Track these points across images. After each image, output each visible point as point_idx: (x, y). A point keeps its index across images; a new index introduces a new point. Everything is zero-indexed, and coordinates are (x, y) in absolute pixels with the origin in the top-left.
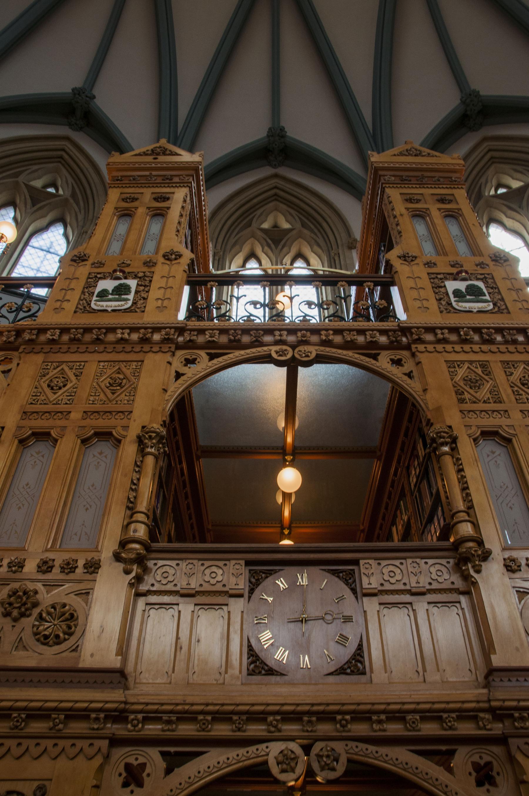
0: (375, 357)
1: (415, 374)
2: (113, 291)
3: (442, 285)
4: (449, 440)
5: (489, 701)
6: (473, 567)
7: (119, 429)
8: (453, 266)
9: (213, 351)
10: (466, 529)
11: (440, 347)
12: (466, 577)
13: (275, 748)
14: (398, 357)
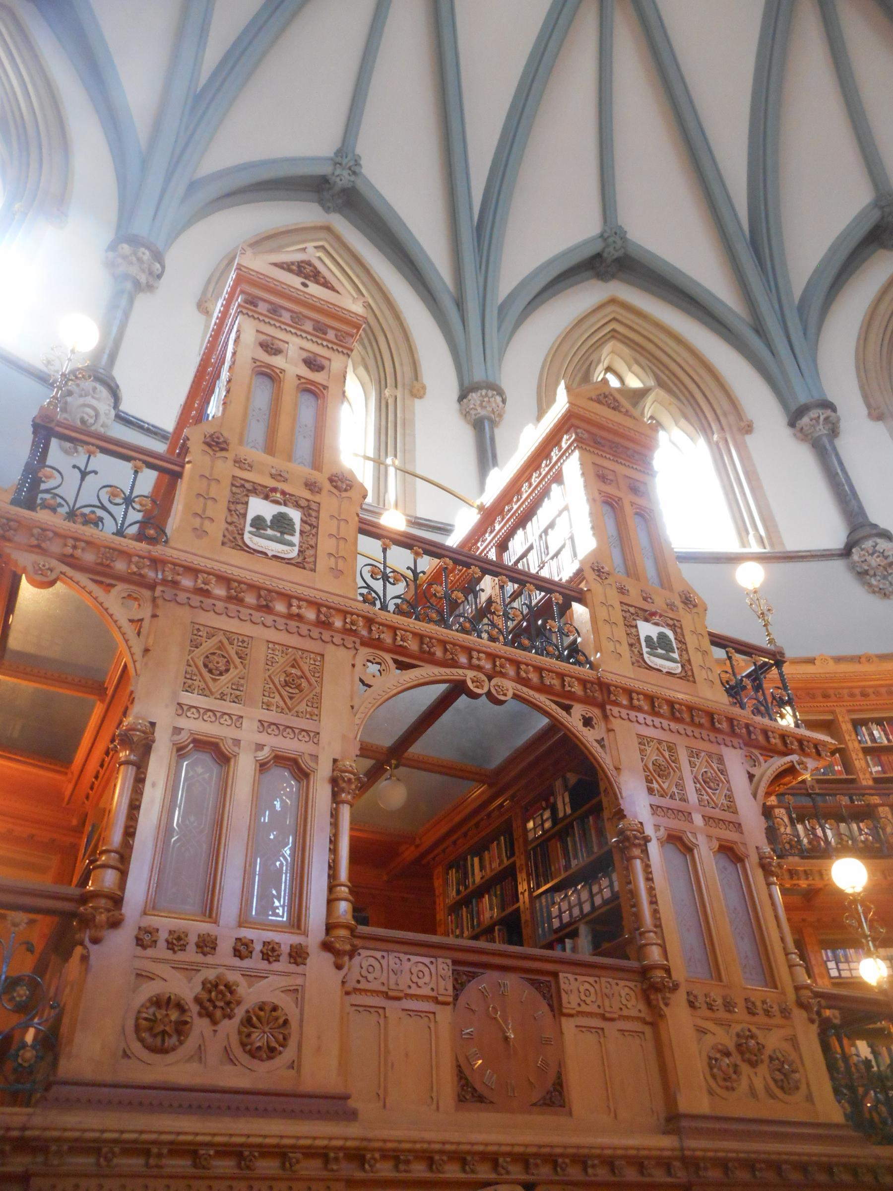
0: (567, 709)
1: (606, 743)
2: (272, 521)
3: (634, 623)
4: (642, 842)
5: (682, 1149)
6: (663, 999)
7: (307, 758)
8: (645, 599)
9: (400, 658)
10: (655, 954)
11: (633, 714)
14: (590, 715)
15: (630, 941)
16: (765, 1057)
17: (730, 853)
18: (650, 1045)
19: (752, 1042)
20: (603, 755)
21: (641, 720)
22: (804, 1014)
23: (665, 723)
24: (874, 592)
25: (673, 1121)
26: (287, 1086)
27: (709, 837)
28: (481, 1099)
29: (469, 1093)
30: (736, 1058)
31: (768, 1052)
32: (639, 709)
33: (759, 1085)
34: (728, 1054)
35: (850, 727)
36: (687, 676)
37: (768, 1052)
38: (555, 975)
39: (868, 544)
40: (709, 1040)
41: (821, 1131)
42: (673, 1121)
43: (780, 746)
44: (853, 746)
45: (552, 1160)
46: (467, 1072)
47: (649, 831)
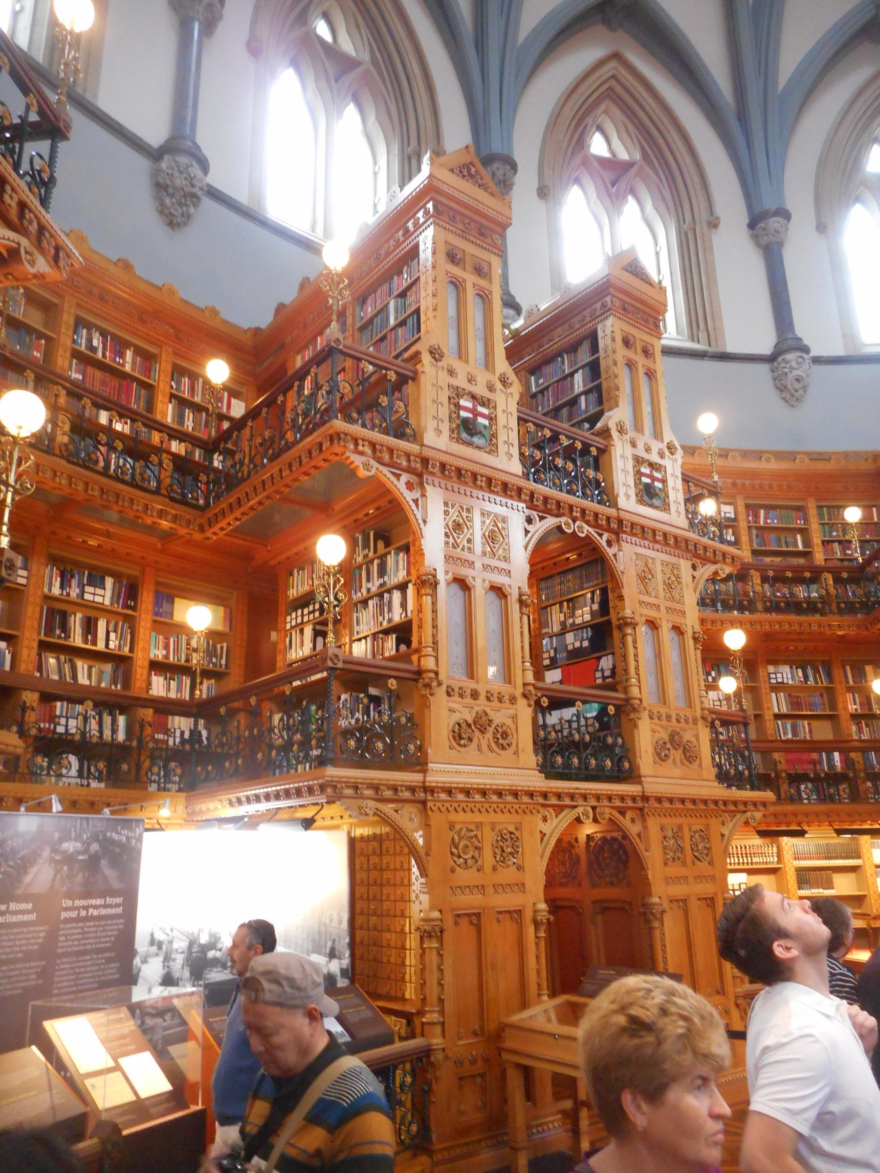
24: (162, 213)
35: (72, 322)
39: (183, 160)
44: (65, 339)
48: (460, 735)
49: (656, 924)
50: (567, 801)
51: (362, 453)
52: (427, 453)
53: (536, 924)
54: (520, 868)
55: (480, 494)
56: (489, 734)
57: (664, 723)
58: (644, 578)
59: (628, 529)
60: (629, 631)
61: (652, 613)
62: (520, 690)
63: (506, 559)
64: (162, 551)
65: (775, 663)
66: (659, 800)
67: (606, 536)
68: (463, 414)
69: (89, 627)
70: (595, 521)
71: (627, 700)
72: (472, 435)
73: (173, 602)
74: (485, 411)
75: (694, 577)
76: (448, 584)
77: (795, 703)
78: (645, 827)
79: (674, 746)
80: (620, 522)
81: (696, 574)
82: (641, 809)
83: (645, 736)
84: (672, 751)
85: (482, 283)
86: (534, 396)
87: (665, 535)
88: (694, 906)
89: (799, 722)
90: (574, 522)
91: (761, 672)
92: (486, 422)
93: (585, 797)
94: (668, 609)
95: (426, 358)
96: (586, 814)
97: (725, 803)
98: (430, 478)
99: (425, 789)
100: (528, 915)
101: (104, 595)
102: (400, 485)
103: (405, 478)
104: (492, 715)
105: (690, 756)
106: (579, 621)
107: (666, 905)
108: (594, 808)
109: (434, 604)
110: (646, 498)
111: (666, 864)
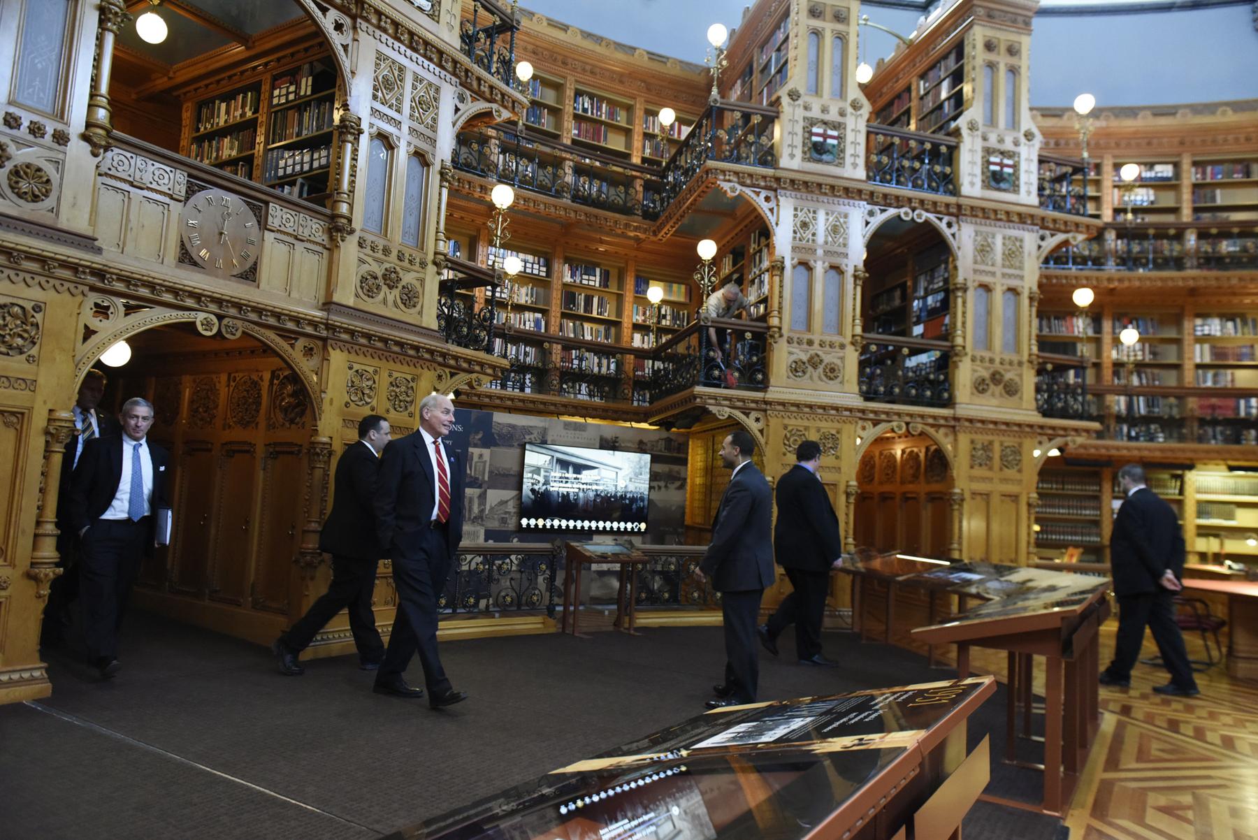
10: (344, 208)
11: (378, 33)
12: (332, 239)
13: (201, 316)
15: (330, 196)
16: (400, 287)
17: (421, 158)
18: (325, 262)
19: (393, 275)
20: (344, 58)
21: (383, 40)
22: (435, 268)
23: (403, 48)
25: (328, 305)
26: (48, 222)
27: (409, 144)
28: (195, 264)
29: (186, 257)
30: (381, 282)
31: (403, 283)
32: (385, 31)
33: (390, 298)
34: (376, 278)
36: (434, 16)
37: (403, 283)
38: (267, 203)
40: (366, 267)
41: (426, 332)
42: (328, 305)
43: (488, 95)
44: (568, 109)
45: (238, 306)
46: (188, 246)
47: (364, 125)
48: (797, 369)
49: (956, 507)
50: (883, 417)
51: (729, 181)
52: (779, 173)
53: (848, 495)
54: (837, 458)
55: (825, 199)
56: (820, 369)
57: (987, 364)
58: (984, 250)
59: (968, 212)
60: (960, 294)
61: (986, 279)
62: (849, 339)
63: (845, 245)
64: (637, 249)
65: (1205, 316)
66: (971, 421)
67: (946, 219)
68: (815, 139)
69: (588, 301)
70: (934, 207)
71: (953, 347)
72: (821, 154)
73: (648, 284)
74: (835, 133)
75: (1040, 247)
76: (794, 267)
77: (1218, 353)
78: (956, 440)
79: (993, 382)
80: (959, 207)
81: (1043, 244)
82: (954, 427)
83: (964, 374)
84: (992, 386)
85: (840, 27)
86: (922, 98)
87: (1008, 213)
88: (995, 500)
89: (1222, 371)
90: (913, 211)
91: (1187, 325)
92: (835, 142)
93: (899, 414)
94: (1004, 275)
95: (785, 101)
96: (900, 428)
97: (1042, 427)
98: (783, 192)
99: (766, 403)
100: (842, 487)
101: (595, 281)
102: (760, 202)
103: (764, 194)
104: (823, 356)
105: (1011, 390)
106: (936, 286)
107: (967, 495)
108: (907, 424)
109: (781, 281)
110: (993, 183)
111: (972, 467)
